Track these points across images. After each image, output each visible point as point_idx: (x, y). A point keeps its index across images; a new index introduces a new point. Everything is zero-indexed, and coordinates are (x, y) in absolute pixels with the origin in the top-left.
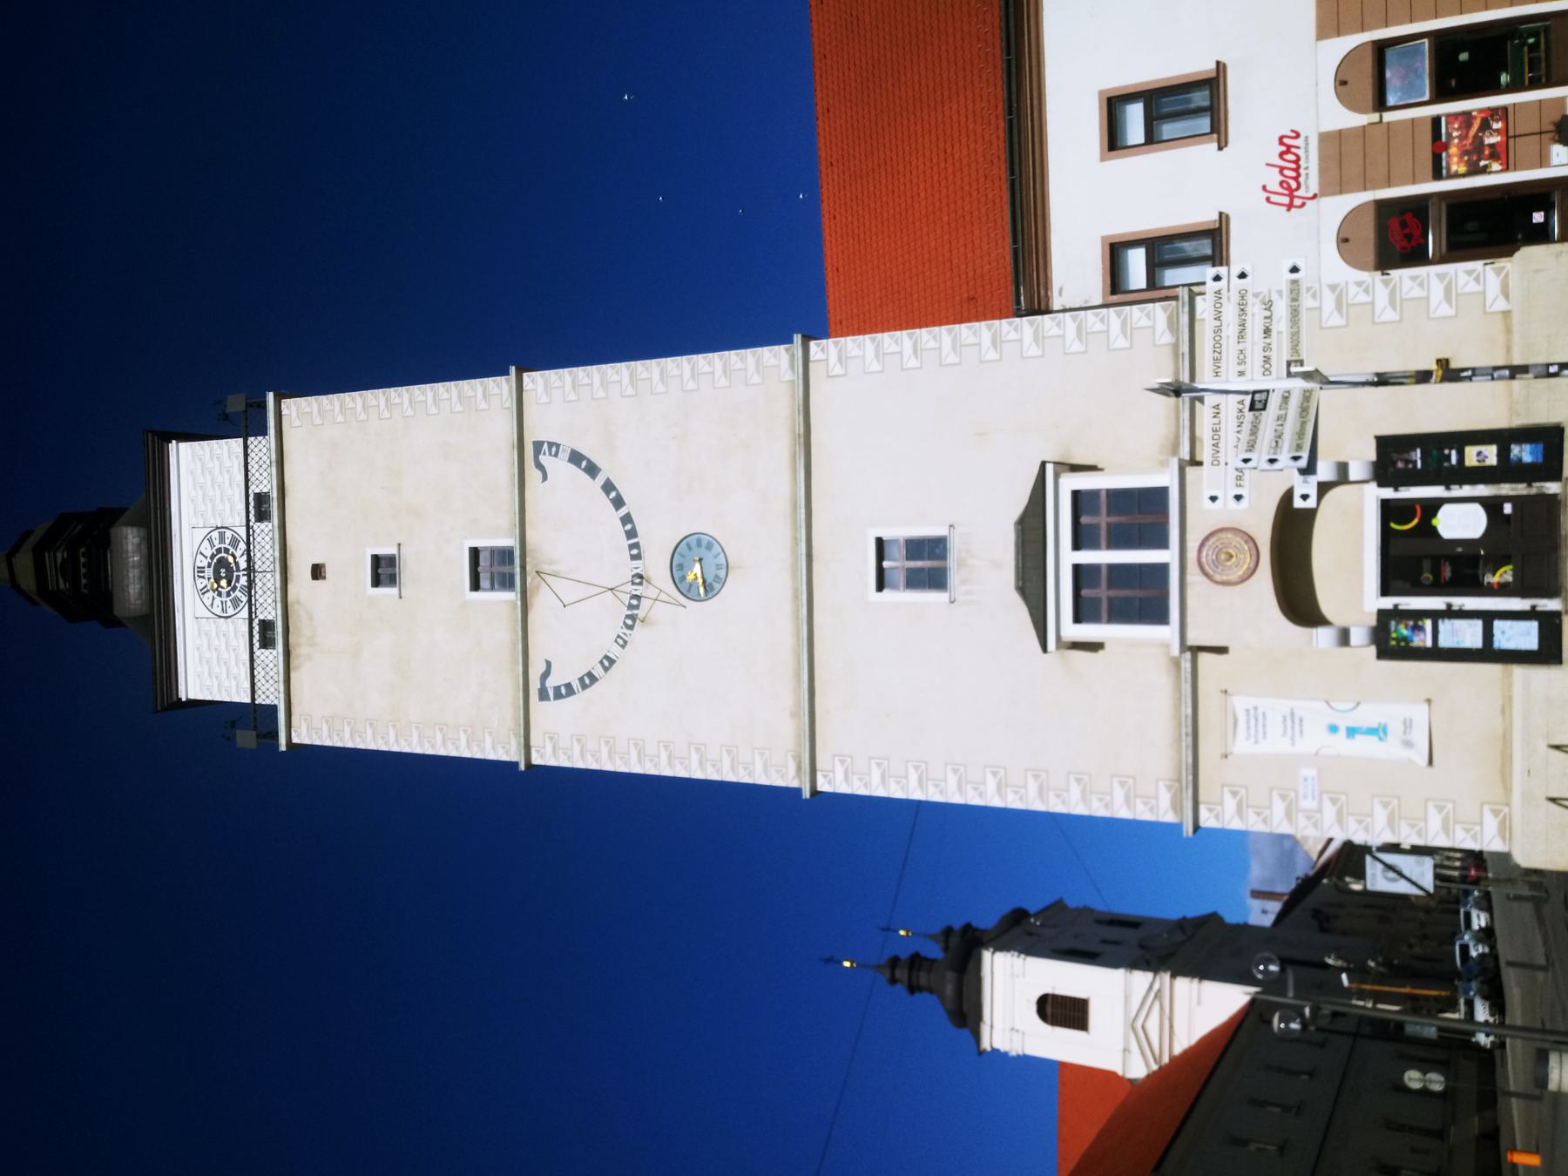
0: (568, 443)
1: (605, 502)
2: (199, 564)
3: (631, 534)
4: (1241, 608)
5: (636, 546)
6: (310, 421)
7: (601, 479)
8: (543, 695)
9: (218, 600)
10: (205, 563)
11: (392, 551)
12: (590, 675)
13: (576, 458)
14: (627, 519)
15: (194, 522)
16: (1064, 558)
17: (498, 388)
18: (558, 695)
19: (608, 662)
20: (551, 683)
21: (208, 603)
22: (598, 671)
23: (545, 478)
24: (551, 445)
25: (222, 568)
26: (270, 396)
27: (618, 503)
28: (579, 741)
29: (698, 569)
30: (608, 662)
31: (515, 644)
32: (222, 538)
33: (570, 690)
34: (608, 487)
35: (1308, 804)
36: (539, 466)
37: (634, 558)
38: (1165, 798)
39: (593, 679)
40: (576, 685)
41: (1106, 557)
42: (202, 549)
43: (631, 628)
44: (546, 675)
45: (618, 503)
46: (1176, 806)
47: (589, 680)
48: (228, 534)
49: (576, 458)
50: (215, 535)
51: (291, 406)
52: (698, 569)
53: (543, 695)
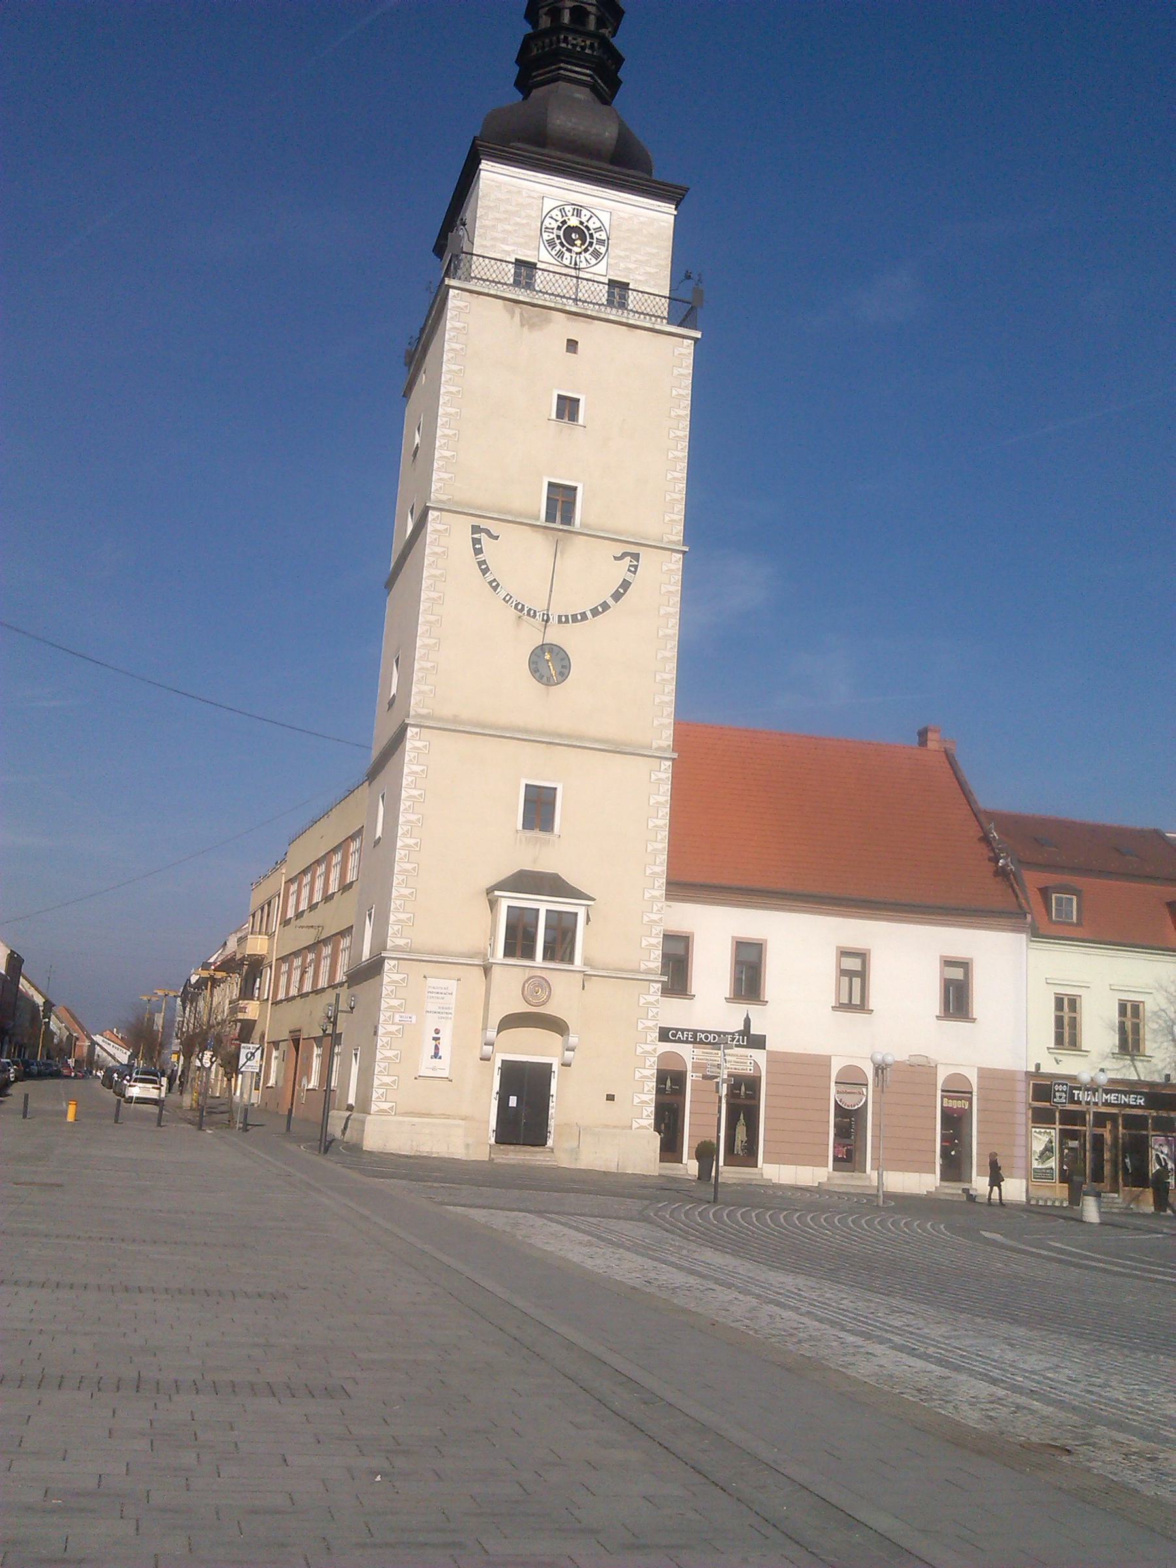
0: (637, 581)
1: (596, 602)
2: (584, 212)
4: (509, 996)
5: (567, 621)
6: (673, 359)
7: (611, 602)
8: (476, 529)
9: (555, 225)
10: (584, 219)
11: (581, 420)
12: (487, 569)
13: (626, 585)
14: (584, 617)
15: (614, 217)
17: (676, 533)
18: (476, 541)
19: (495, 586)
20: (483, 536)
21: (553, 214)
23: (616, 558)
24: (636, 567)
26: (699, 336)
27: (595, 612)
28: (444, 552)
29: (549, 664)
30: (495, 586)
31: (510, 513)
32: (601, 242)
33: (478, 552)
34: (605, 606)
35: (397, 1018)
37: (560, 617)
38: (401, 942)
41: (539, 930)
42: (594, 219)
43: (516, 608)
45: (595, 612)
46: (397, 948)
49: (626, 585)
50: (604, 237)
51: (687, 348)
52: (549, 664)
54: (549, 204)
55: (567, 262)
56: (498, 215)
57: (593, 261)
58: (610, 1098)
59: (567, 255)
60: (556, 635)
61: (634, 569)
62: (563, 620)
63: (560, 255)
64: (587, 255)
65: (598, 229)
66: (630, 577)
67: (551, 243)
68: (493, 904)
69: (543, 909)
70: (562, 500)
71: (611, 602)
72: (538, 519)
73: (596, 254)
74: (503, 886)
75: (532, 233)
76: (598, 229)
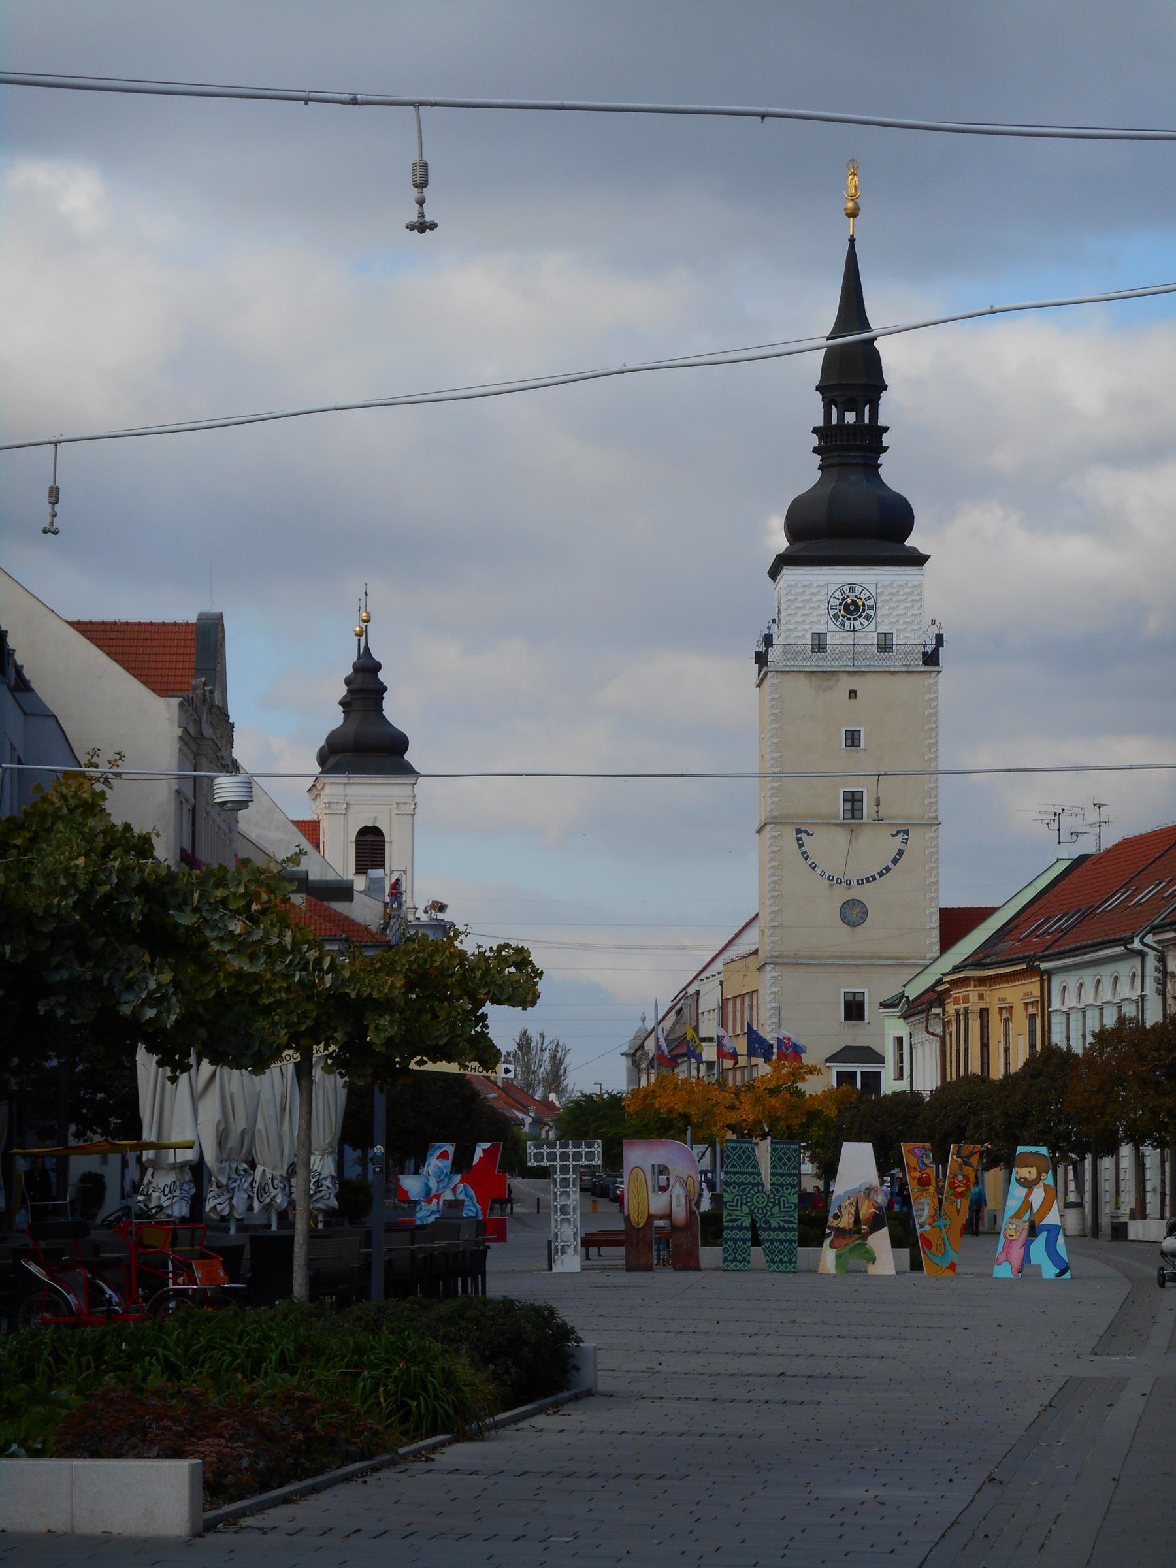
0: (907, 848)
3: (868, 881)
7: (891, 865)
8: (798, 831)
9: (837, 603)
13: (901, 852)
14: (874, 878)
18: (799, 839)
19: (813, 867)
20: (803, 835)
21: (836, 595)
22: (809, 861)
25: (852, 609)
27: (881, 874)
29: (853, 913)
32: (870, 608)
33: (801, 846)
34: (888, 869)
39: (806, 858)
40: (803, 849)
44: (806, 832)
45: (881, 874)
48: (872, 613)
49: (901, 852)
52: (853, 913)
54: (832, 588)
55: (847, 628)
56: (798, 605)
57: (866, 623)
59: (847, 622)
60: (856, 893)
62: (860, 882)
63: (843, 624)
64: (862, 620)
65: (868, 599)
66: (902, 847)
67: (836, 617)
71: (891, 865)
72: (838, 817)
73: (868, 618)
75: (822, 612)
76: (868, 599)
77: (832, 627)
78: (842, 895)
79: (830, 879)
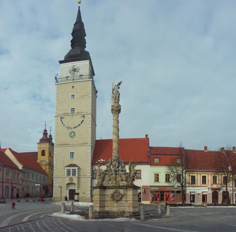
3: (76, 127)
8: (61, 118)
13: (83, 121)
16: (71, 168)
22: (63, 124)
25: (74, 70)
27: (78, 126)
29: (72, 135)
32: (78, 70)
33: (62, 121)
34: (80, 125)
36: (82, 116)
45: (78, 126)
47: (62, 123)
48: (78, 70)
49: (83, 121)
52: (72, 135)
53: (61, 118)
58: (84, 193)
60: (73, 130)
61: (84, 118)
63: (72, 74)
66: (83, 119)
67: (71, 72)
68: (65, 169)
69: (71, 169)
70: (73, 110)
73: (77, 72)
74: (67, 166)
77: (70, 75)
78: (70, 131)
79: (68, 128)
